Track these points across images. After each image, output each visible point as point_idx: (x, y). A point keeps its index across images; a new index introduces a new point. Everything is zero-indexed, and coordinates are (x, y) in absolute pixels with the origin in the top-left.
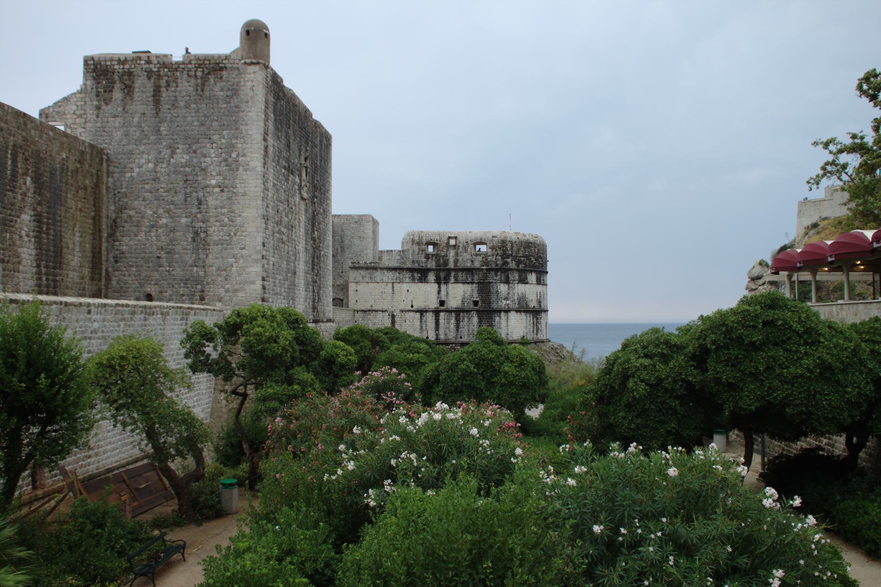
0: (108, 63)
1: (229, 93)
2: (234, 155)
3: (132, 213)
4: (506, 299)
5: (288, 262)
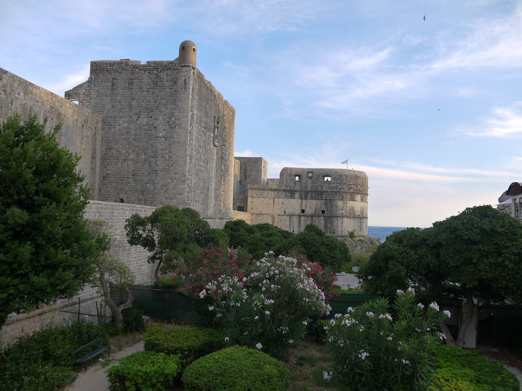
0: (104, 66)
1: (172, 83)
2: (173, 119)
3: (114, 152)
4: (342, 210)
5: (204, 183)
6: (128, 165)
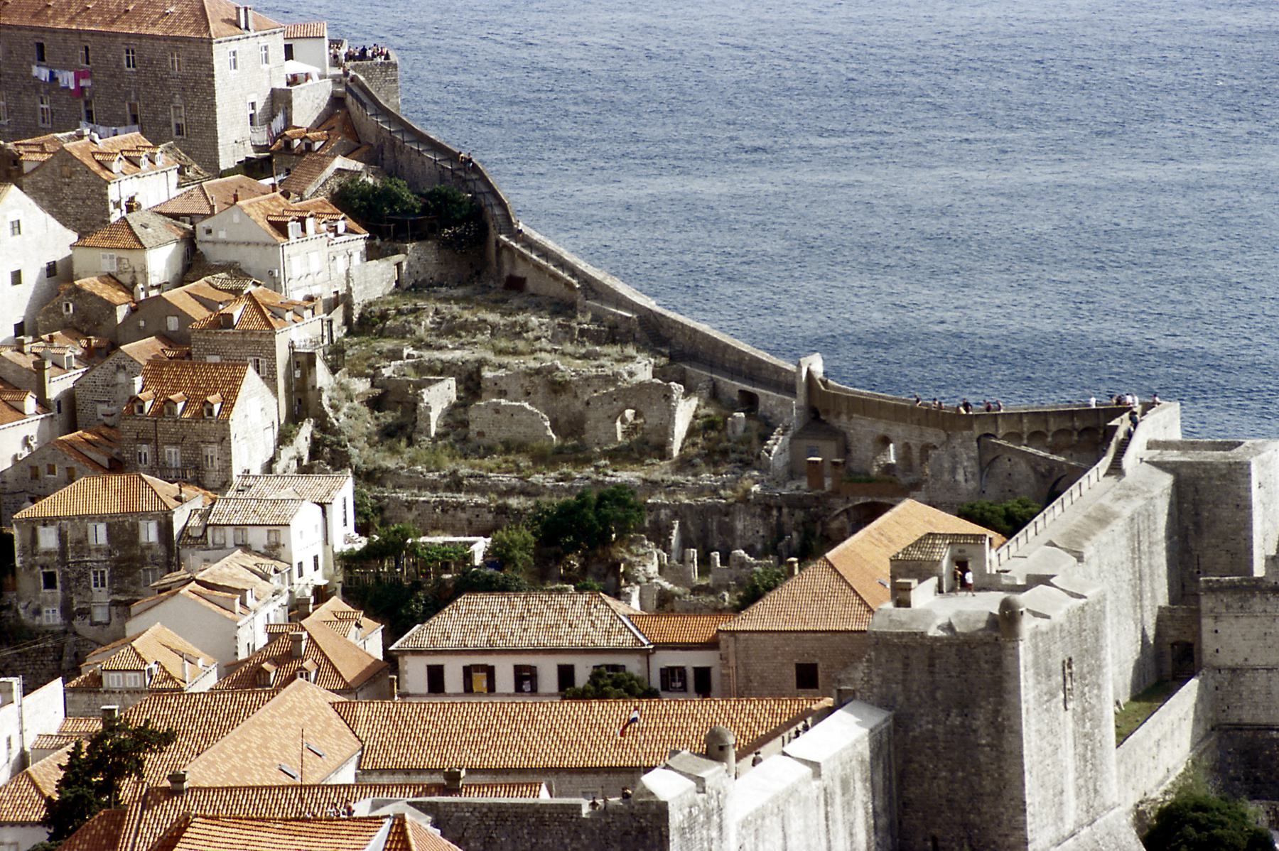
3: (916, 766)
6: (939, 786)
